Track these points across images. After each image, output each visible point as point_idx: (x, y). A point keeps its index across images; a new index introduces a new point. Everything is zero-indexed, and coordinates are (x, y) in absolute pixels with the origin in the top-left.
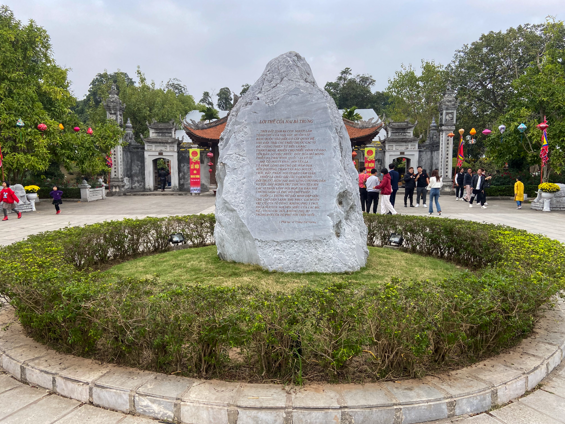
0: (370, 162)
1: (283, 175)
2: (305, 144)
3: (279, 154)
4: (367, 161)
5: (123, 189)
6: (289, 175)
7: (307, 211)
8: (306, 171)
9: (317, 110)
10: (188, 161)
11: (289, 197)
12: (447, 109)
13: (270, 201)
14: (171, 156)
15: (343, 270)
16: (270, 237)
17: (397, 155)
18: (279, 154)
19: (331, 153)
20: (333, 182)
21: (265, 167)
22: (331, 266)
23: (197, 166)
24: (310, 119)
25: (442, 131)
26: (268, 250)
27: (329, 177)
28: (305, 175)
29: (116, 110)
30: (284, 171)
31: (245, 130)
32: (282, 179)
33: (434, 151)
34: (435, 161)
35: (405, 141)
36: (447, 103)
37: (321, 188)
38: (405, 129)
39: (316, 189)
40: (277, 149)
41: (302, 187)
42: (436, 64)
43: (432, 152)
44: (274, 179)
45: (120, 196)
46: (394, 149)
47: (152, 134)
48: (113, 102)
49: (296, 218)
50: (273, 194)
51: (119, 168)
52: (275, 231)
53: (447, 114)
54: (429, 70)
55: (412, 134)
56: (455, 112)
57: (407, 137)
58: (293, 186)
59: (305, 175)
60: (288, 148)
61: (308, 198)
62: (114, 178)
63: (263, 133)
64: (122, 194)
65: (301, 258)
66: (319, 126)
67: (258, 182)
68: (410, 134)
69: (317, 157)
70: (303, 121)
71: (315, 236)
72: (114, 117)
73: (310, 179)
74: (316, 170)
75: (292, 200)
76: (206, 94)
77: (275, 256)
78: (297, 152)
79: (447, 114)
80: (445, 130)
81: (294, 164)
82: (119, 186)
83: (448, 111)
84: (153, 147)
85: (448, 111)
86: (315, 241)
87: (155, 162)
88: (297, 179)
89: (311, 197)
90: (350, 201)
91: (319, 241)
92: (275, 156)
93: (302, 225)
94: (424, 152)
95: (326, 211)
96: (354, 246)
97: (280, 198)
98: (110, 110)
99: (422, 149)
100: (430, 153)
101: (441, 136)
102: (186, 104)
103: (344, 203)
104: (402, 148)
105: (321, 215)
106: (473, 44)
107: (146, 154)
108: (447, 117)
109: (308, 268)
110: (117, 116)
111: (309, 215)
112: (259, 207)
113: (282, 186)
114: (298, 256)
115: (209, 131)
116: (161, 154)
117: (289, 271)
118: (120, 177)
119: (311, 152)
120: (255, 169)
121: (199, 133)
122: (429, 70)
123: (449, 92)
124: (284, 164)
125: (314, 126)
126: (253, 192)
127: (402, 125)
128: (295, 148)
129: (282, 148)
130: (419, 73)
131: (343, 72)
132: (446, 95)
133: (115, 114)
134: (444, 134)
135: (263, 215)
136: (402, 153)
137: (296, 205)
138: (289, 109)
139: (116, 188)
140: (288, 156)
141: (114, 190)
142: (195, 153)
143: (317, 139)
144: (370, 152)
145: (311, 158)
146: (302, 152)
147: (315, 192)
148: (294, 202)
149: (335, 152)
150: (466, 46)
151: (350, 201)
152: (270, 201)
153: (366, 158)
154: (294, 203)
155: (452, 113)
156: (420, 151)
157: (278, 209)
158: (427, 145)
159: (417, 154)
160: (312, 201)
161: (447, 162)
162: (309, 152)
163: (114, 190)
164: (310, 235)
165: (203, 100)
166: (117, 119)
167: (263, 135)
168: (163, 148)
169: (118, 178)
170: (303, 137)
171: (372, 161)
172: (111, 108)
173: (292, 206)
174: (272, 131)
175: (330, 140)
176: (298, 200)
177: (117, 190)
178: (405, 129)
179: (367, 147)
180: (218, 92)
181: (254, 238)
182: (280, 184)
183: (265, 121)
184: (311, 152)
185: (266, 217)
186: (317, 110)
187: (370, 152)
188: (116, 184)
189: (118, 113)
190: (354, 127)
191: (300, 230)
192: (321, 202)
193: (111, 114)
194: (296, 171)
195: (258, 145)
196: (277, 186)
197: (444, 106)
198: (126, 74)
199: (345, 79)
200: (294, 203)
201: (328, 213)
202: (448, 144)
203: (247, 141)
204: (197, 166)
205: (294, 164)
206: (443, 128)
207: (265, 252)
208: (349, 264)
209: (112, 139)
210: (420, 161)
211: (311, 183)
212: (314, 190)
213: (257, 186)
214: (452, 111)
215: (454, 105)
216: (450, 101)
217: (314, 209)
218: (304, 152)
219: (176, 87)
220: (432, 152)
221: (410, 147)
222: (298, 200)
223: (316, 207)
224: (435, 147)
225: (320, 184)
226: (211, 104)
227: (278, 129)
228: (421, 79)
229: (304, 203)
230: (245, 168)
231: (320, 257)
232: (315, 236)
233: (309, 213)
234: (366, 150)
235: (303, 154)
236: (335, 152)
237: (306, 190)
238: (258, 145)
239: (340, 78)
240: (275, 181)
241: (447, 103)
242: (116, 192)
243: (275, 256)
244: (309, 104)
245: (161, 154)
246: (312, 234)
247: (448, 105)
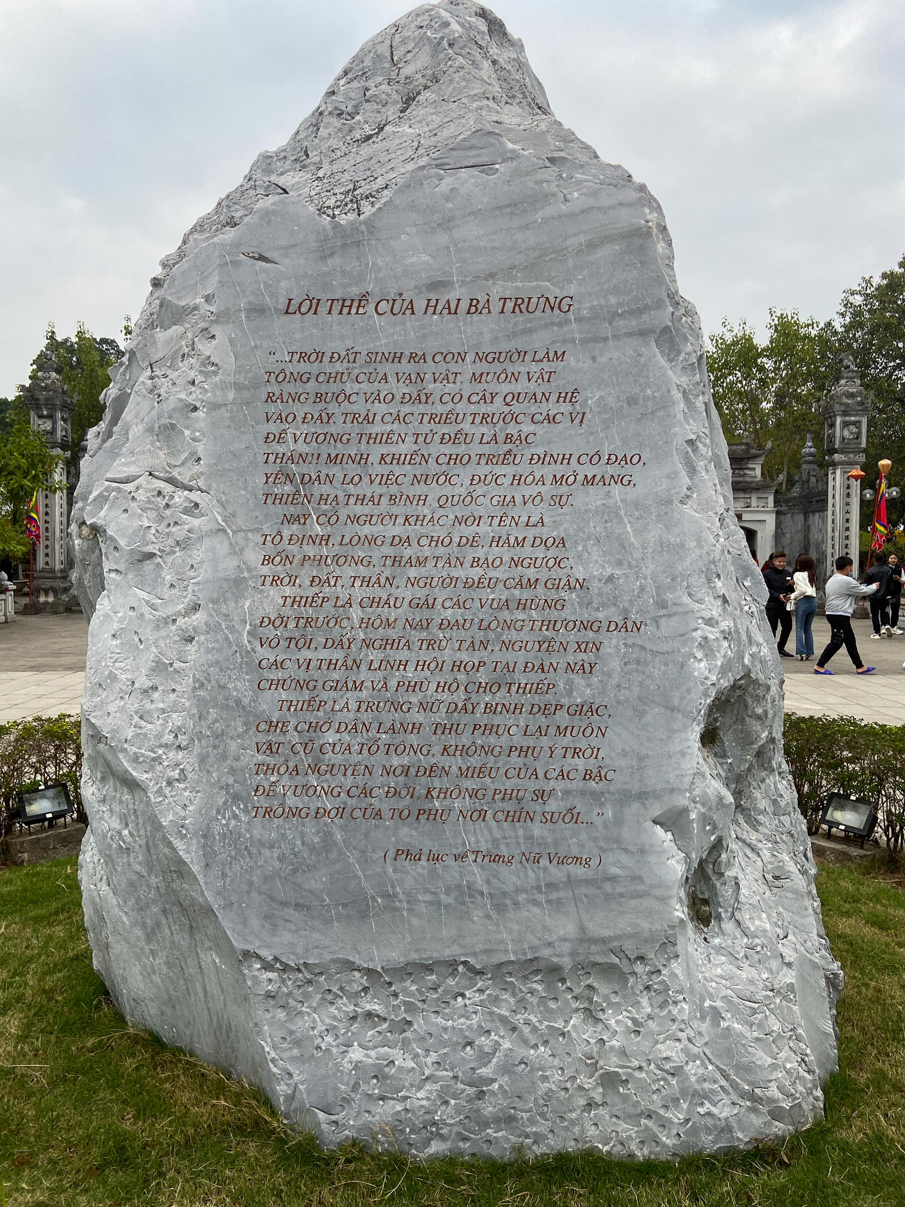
1: (406, 593)
2: (527, 428)
3: (385, 480)
5: (65, 598)
6: (441, 595)
7: (541, 795)
8: (531, 573)
9: (592, 246)
11: (440, 716)
12: (845, 413)
13: (331, 737)
15: (742, 1138)
16: (328, 943)
18: (385, 480)
19: (672, 476)
20: (683, 636)
21: (310, 550)
22: (676, 1116)
24: (554, 292)
25: (834, 464)
26: (318, 1020)
27: (663, 605)
28: (526, 595)
29: (52, 408)
30: (413, 572)
31: (206, 348)
32: (403, 612)
33: (814, 512)
34: (815, 535)
36: (845, 400)
37: (615, 664)
38: (742, 459)
39: (588, 669)
40: (376, 451)
41: (509, 657)
42: (803, 320)
43: (806, 514)
44: (356, 613)
45: (55, 613)
48: (46, 388)
49: (480, 836)
50: (352, 698)
51: (57, 547)
52: (357, 908)
53: (845, 424)
54: (786, 332)
55: (758, 472)
56: (865, 420)
57: (748, 479)
58: (464, 656)
59: (526, 595)
60: (436, 449)
61: (542, 721)
62: (43, 570)
63: (303, 367)
64: (62, 609)
65: (506, 1069)
66: (606, 329)
67: (270, 632)
69: (594, 497)
70: (521, 305)
71: (585, 939)
72: (48, 425)
73: (554, 615)
74: (590, 565)
75: (453, 728)
77: (356, 1054)
78: (483, 470)
79: (845, 424)
80: (842, 463)
81: (469, 531)
82: (55, 591)
83: (847, 419)
85: (847, 419)
86: (587, 967)
88: (485, 614)
89: (562, 718)
90: (756, 726)
91: (608, 971)
92: (365, 489)
93: (510, 877)
94: (789, 516)
95: (642, 796)
96: (788, 977)
97: (389, 717)
98: (38, 408)
99: (784, 508)
100: (801, 517)
101: (830, 477)
103: (727, 739)
105: (619, 821)
106: (884, 276)
108: (846, 433)
109: (542, 1127)
110: (54, 423)
111: (549, 819)
112: (271, 769)
113: (404, 655)
114: (484, 1057)
117: (435, 1147)
118: (58, 566)
119: (559, 469)
120: (254, 557)
122: (786, 332)
123: (850, 374)
124: (412, 530)
125: (574, 330)
126: (241, 686)
128: (476, 449)
129: (403, 449)
130: (762, 339)
132: (843, 382)
133: (50, 417)
134: (838, 472)
135: (295, 813)
137: (475, 761)
138: (442, 238)
139: (47, 595)
140: (434, 491)
141: (42, 599)
143: (591, 398)
145: (558, 501)
146: (509, 470)
147: (583, 690)
148: (465, 740)
149: (692, 471)
150: (868, 282)
151: (756, 726)
152: (331, 737)
154: (465, 751)
155: (857, 424)
156: (778, 513)
157: (378, 779)
158: (794, 498)
159: (771, 520)
160: (567, 740)
161: (847, 538)
162: (548, 471)
163: (42, 599)
164: (557, 931)
166: (54, 429)
167: (301, 378)
169: (53, 571)
170: (521, 386)
172: (42, 402)
173: (454, 763)
174: (352, 355)
175: (665, 404)
176: (491, 729)
177: (51, 599)
178: (742, 459)
181: (239, 945)
182: (387, 643)
183: (314, 305)
184: (559, 469)
185: (310, 827)
186: (592, 246)
188: (48, 584)
189: (59, 415)
191: (500, 903)
192: (617, 744)
193: (41, 417)
194: (476, 573)
195: (274, 428)
196: (375, 655)
197: (837, 407)
198: (113, 341)
200: (465, 751)
201: (656, 810)
202: (848, 495)
203: (215, 407)
205: (469, 531)
206: (837, 457)
207: (300, 1025)
208: (773, 1092)
209: (26, 474)
210: (778, 535)
211: (562, 635)
212: (578, 680)
213: (263, 653)
214: (857, 418)
215: (861, 403)
216: (852, 395)
217: (577, 784)
218: (524, 469)
220: (806, 514)
221: (754, 502)
222: (491, 729)
223: (588, 775)
224: (815, 502)
225: (612, 643)
227: (383, 344)
228: (770, 352)
229: (524, 751)
230: (198, 554)
231: (612, 1064)
232: (585, 939)
233: (553, 805)
235: (518, 480)
236: (692, 471)
237: (535, 677)
238: (274, 428)
240: (365, 623)
241: (845, 400)
242: (47, 603)
243: (356, 1054)
244: (549, 211)
246: (565, 927)
247: (847, 405)
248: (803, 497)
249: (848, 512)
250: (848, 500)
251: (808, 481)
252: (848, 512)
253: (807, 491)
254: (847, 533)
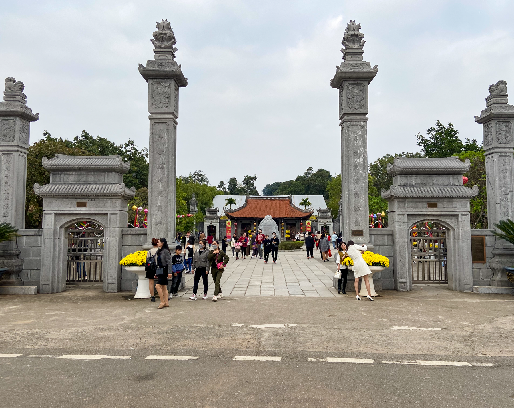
10: (226, 226)
14: (216, 224)
23: (230, 229)
35: (326, 218)
47: (207, 214)
68: (329, 214)
72: (193, 208)
76: (222, 183)
84: (208, 220)
87: (209, 227)
102: (214, 193)
104: (325, 221)
107: (205, 223)
115: (235, 213)
116: (211, 223)
121: (231, 214)
131: (308, 170)
136: (325, 224)
142: (229, 223)
144: (309, 223)
159: (332, 224)
165: (219, 187)
168: (213, 221)
171: (309, 227)
180: (229, 181)
187: (309, 223)
199: (309, 174)
204: (230, 229)
219: (199, 175)
226: (225, 188)
239: (306, 173)
245: (211, 223)
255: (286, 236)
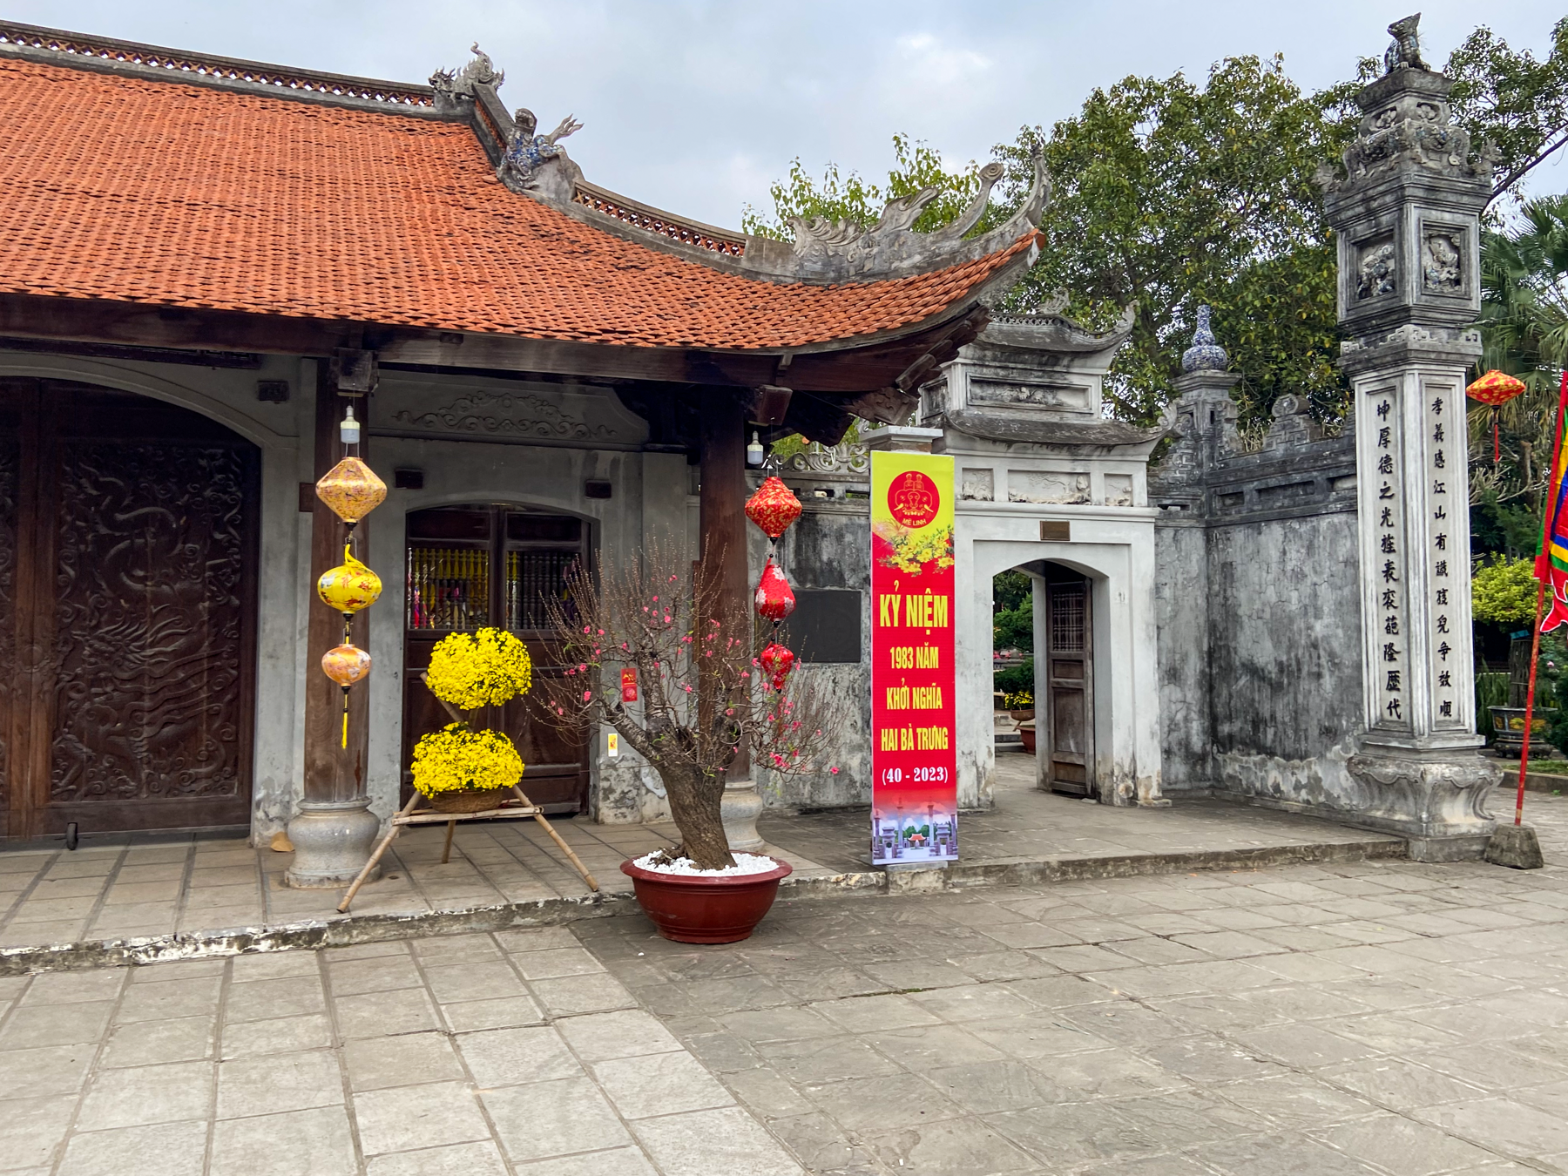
0: (912, 585)
4: (887, 579)
17: (1021, 544)
25: (1402, 357)
33: (1254, 523)
46: (1001, 499)
57: (1072, 419)
83: (1435, 215)
85: (1435, 215)
101: (1365, 409)
104: (1053, 498)
127: (1028, 335)
134: (1411, 385)
136: (1055, 531)
153: (881, 548)
159: (1143, 540)
179: (885, 443)
190: (752, 275)
206: (1412, 334)
221: (1098, 487)
234: (885, 468)
248: (1199, 482)
249: (1440, 515)
250: (1440, 475)
251: (1214, 436)
252: (1440, 515)
253: (1208, 466)
254: (1442, 582)
255: (442, 763)
